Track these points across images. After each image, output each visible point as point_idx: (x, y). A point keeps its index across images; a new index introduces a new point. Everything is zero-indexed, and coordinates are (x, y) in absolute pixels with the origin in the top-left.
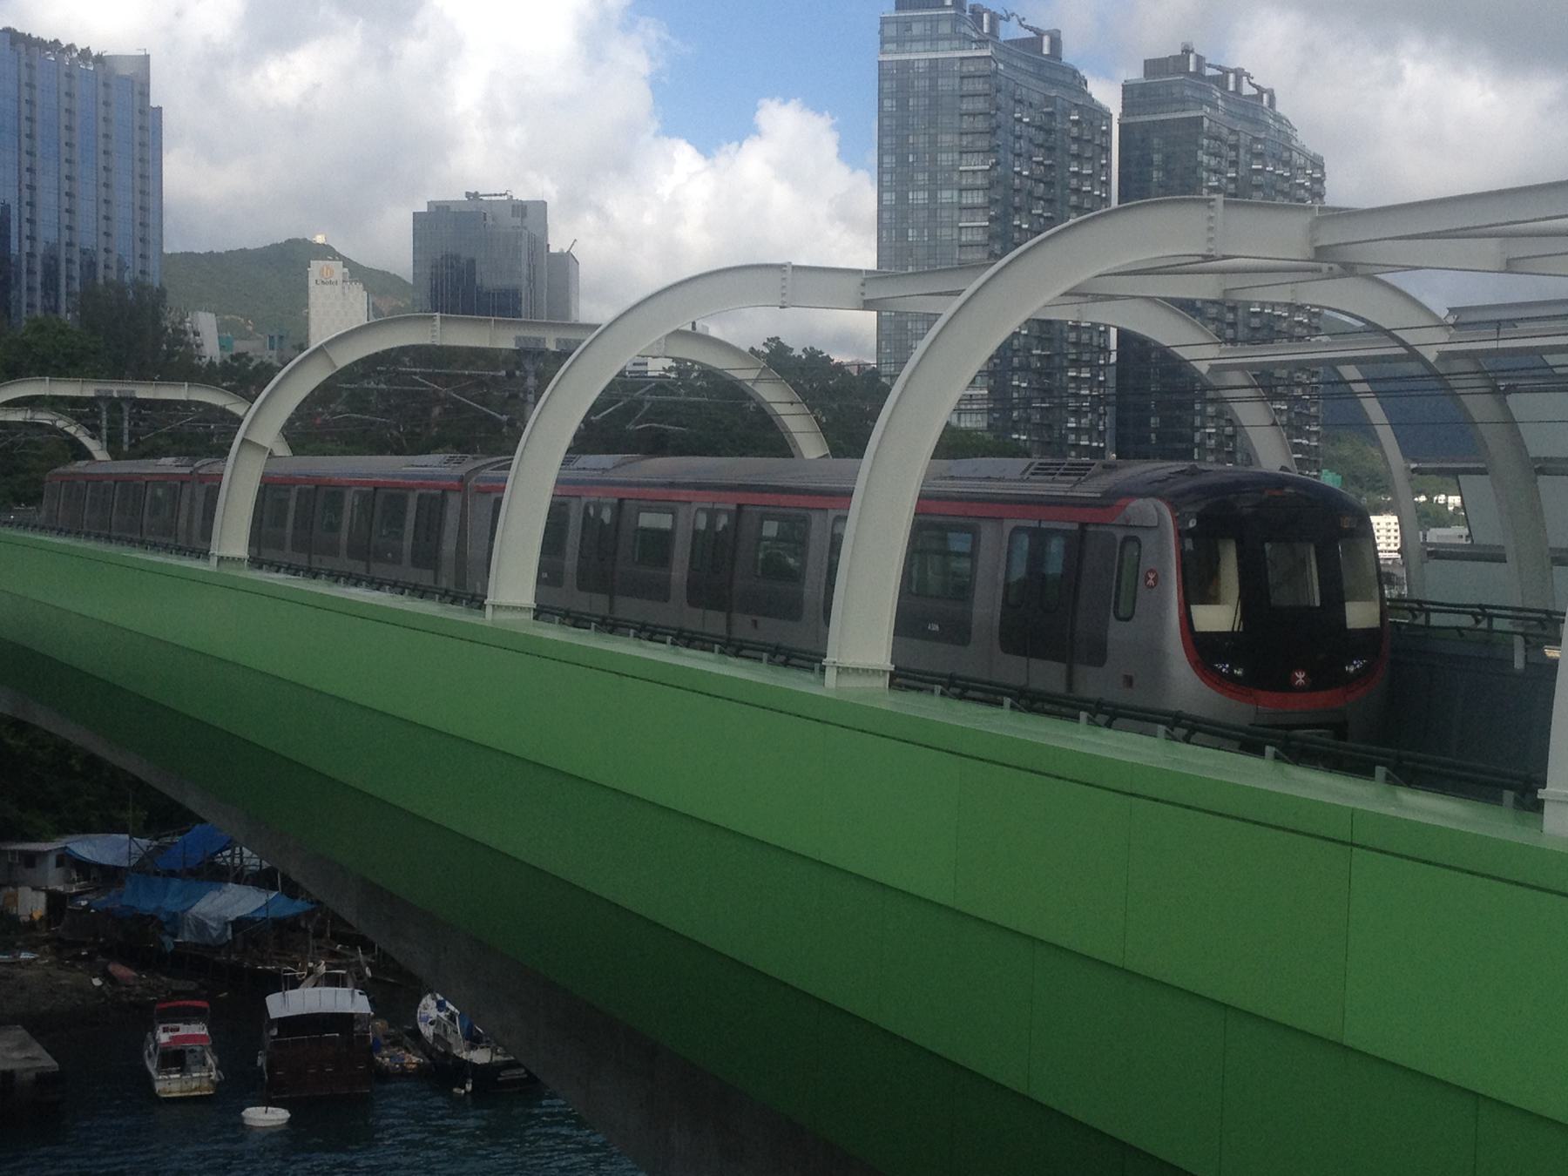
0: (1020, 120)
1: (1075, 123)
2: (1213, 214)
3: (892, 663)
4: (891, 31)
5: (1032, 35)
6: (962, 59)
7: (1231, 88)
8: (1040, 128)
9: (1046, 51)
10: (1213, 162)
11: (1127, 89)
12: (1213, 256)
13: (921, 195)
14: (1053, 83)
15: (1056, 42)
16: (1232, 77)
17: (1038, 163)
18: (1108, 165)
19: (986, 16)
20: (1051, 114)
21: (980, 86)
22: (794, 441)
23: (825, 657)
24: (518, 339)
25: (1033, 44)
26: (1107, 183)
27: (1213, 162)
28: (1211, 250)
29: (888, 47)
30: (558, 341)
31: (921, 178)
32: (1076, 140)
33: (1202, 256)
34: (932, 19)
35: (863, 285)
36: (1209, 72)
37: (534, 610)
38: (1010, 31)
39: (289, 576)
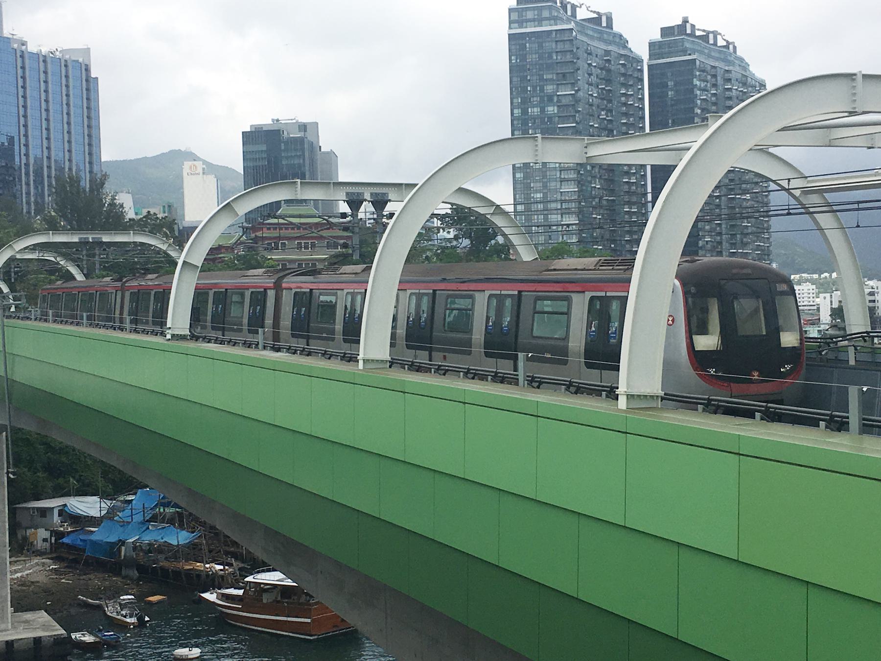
2: (854, 85)
4: (515, 16)
5: (597, 16)
7: (711, 42)
8: (601, 69)
9: (604, 24)
11: (652, 45)
12: (856, 112)
13: (535, 110)
15: (609, 19)
16: (711, 36)
18: (642, 89)
19: (569, 7)
20: (608, 61)
21: (567, 47)
24: (347, 194)
25: (597, 21)
26: (642, 99)
28: (855, 108)
29: (513, 25)
30: (372, 194)
31: (536, 99)
32: (624, 75)
33: (850, 112)
36: (698, 33)
37: (390, 362)
38: (582, 14)
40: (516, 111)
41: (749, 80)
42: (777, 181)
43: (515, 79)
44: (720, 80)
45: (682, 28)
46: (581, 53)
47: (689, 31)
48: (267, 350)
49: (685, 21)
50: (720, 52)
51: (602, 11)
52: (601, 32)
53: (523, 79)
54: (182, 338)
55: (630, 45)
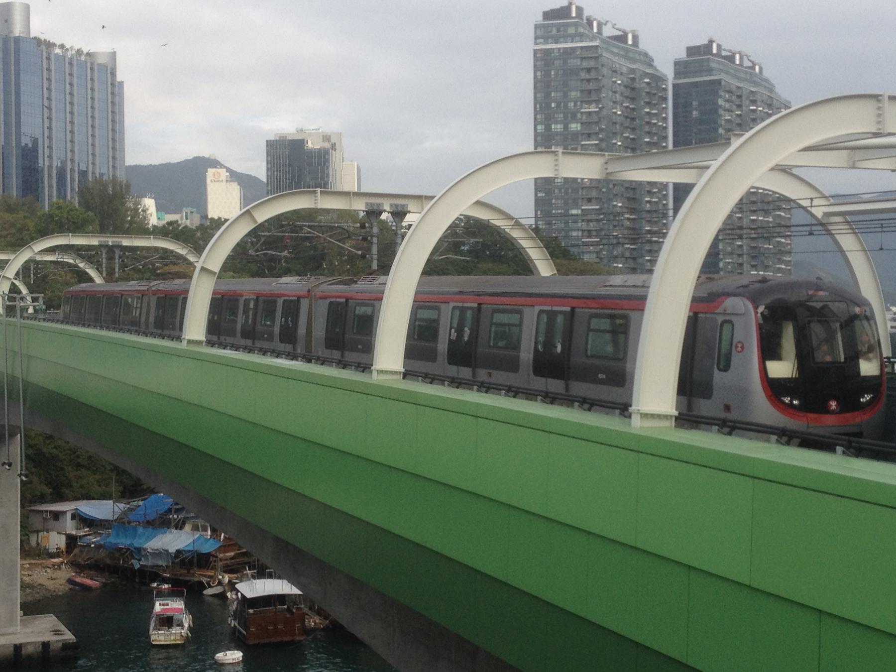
0: (615, 82)
1: (648, 84)
2: (881, 105)
3: (676, 410)
5: (622, 33)
6: (582, 48)
7: (738, 62)
8: (626, 87)
9: (630, 42)
10: (727, 106)
11: (677, 64)
12: (881, 133)
13: (559, 126)
14: (634, 61)
15: (635, 38)
16: (737, 57)
17: (627, 107)
18: (666, 108)
19: (595, 24)
20: (633, 79)
21: (592, 64)
22: (535, 266)
23: (631, 406)
24: (367, 204)
25: (622, 38)
27: (727, 106)
28: (880, 129)
29: (538, 41)
30: (391, 205)
32: (648, 93)
34: (564, 25)
35: (606, 163)
36: (724, 53)
38: (608, 32)
39: (234, 352)
40: (539, 127)
41: (775, 102)
42: (798, 201)
43: (539, 95)
44: (746, 102)
45: (707, 48)
46: (605, 71)
47: (715, 51)
48: (282, 358)
49: (711, 42)
50: (746, 73)
51: (628, 29)
52: (627, 51)
53: (547, 95)
54: (199, 343)
55: (656, 63)
